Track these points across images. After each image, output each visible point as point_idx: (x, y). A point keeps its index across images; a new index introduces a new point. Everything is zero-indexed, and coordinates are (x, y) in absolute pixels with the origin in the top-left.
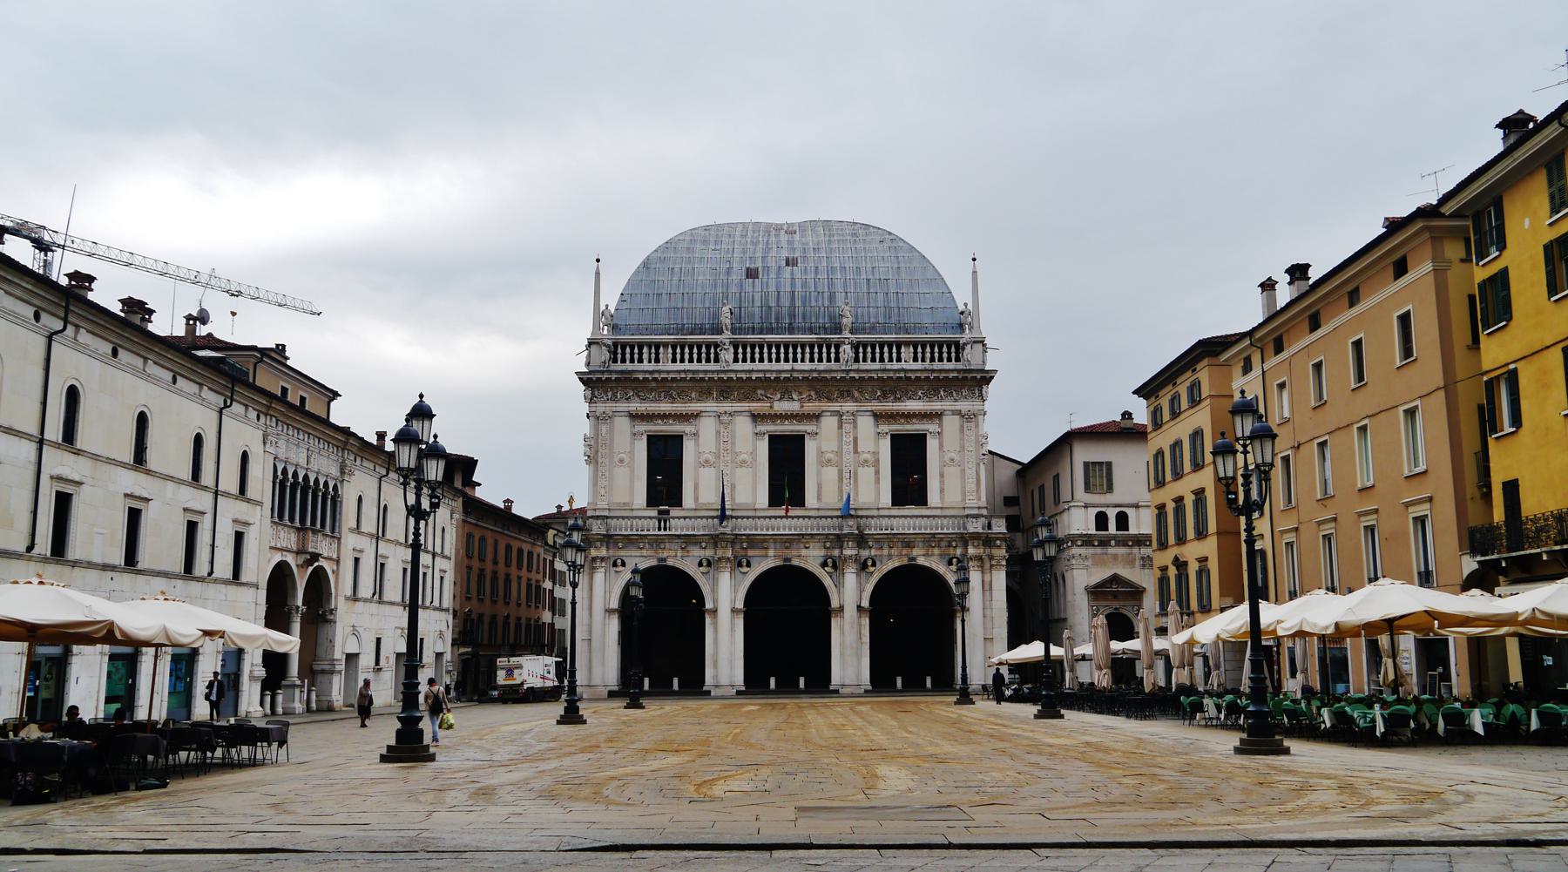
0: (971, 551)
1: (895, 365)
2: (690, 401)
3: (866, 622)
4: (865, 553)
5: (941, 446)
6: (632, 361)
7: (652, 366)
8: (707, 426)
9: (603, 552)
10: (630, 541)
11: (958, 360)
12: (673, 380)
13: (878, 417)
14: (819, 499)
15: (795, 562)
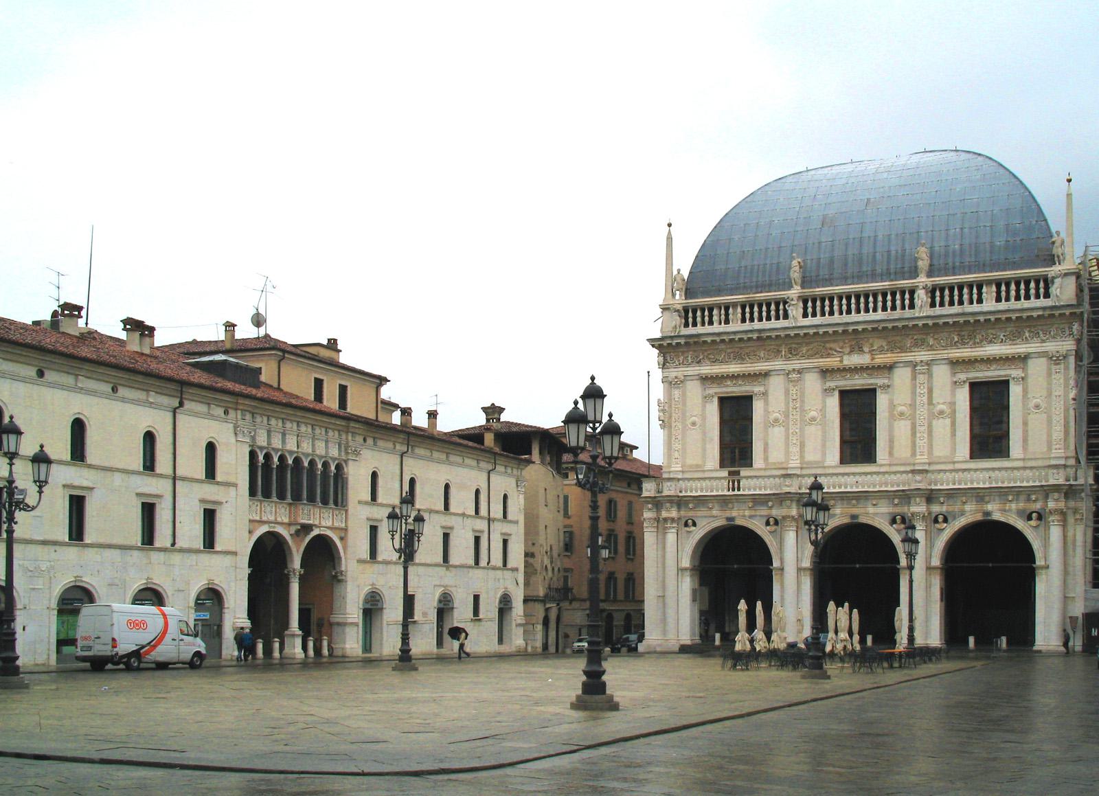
1: (975, 308)
2: (760, 359)
5: (1025, 391)
6: (760, 319)
7: (723, 328)
8: (776, 385)
9: (674, 514)
10: (701, 501)
11: (1047, 295)
12: (741, 340)
13: (955, 364)
14: (891, 454)
15: (863, 520)
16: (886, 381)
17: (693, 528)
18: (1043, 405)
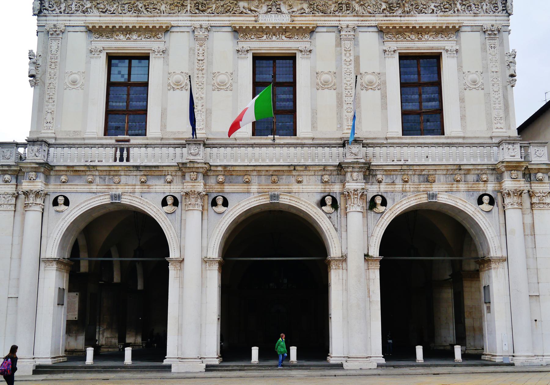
0: (508, 184)
3: (375, 275)
4: (373, 190)
5: (460, 67)
8: (179, 44)
10: (74, 171)
13: (381, 31)
14: (314, 127)
15: (285, 200)
16: (308, 46)
17: (62, 207)
18: (480, 80)
